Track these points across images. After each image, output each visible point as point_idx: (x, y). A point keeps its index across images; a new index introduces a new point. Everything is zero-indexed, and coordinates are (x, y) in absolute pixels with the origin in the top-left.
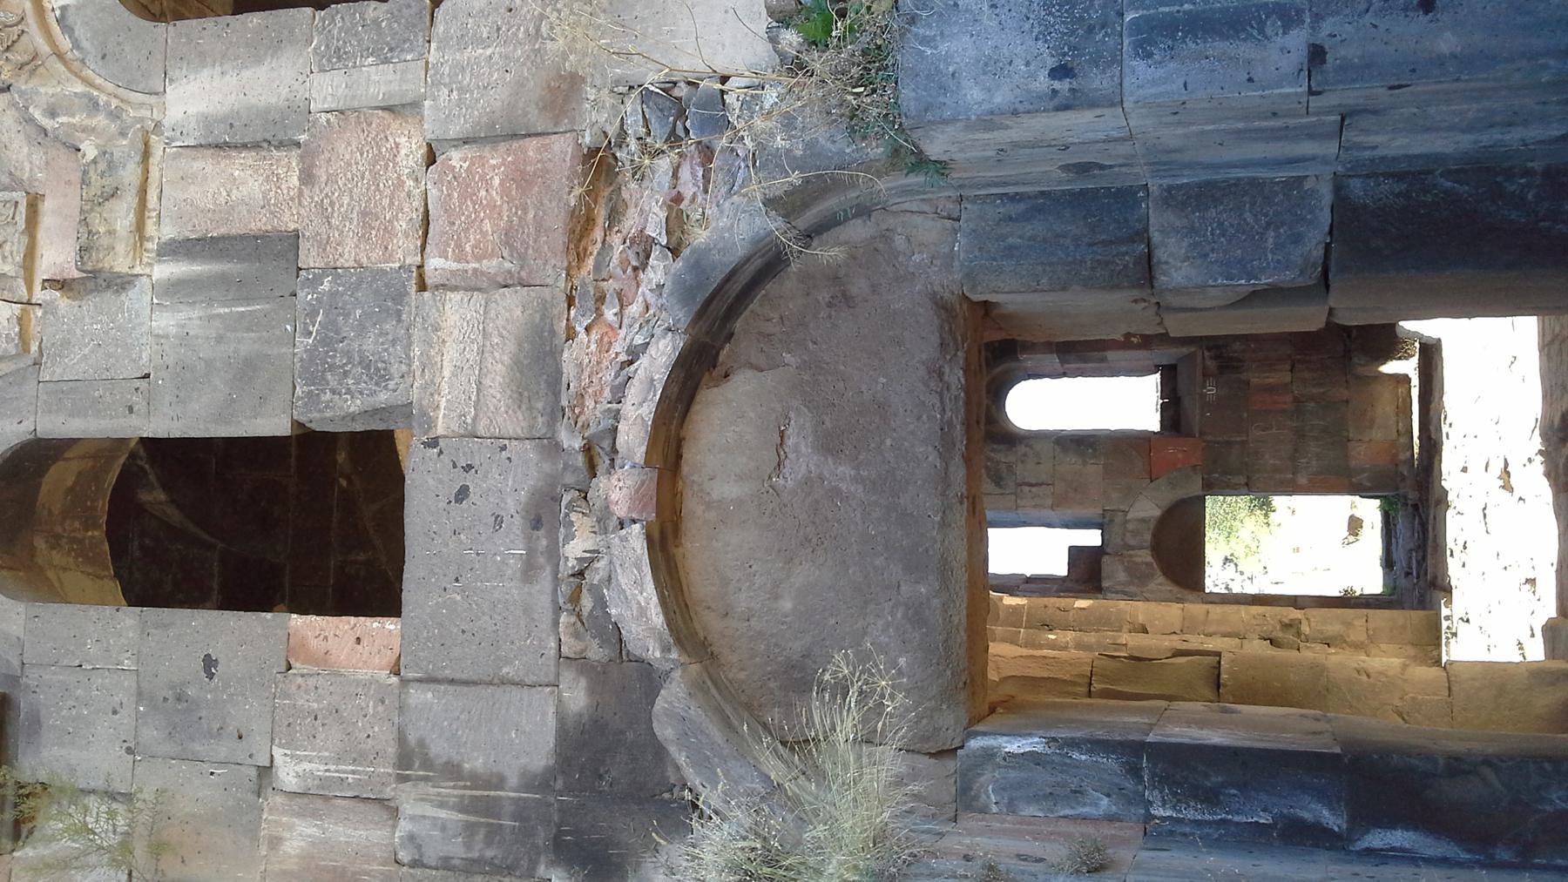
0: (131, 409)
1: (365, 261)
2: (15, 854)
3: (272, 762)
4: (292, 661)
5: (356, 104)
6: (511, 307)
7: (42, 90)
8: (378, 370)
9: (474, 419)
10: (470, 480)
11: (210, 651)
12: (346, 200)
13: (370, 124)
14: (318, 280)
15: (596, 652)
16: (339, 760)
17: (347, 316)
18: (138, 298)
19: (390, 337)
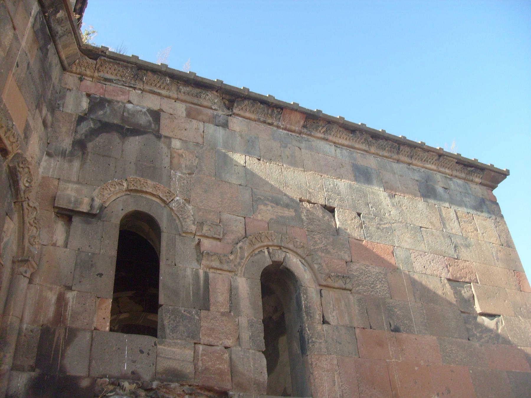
0: (167, 260)
1: (202, 328)
2: (53, 213)
3: (73, 290)
4: (100, 299)
5: (240, 329)
6: (189, 369)
7: (246, 246)
9: (161, 357)
10: (145, 354)
11: (104, 275)
12: (217, 324)
13: (235, 332)
14: (198, 315)
15: (97, 388)
16: (72, 310)
17: (189, 322)
18: (195, 265)
19: (183, 334)
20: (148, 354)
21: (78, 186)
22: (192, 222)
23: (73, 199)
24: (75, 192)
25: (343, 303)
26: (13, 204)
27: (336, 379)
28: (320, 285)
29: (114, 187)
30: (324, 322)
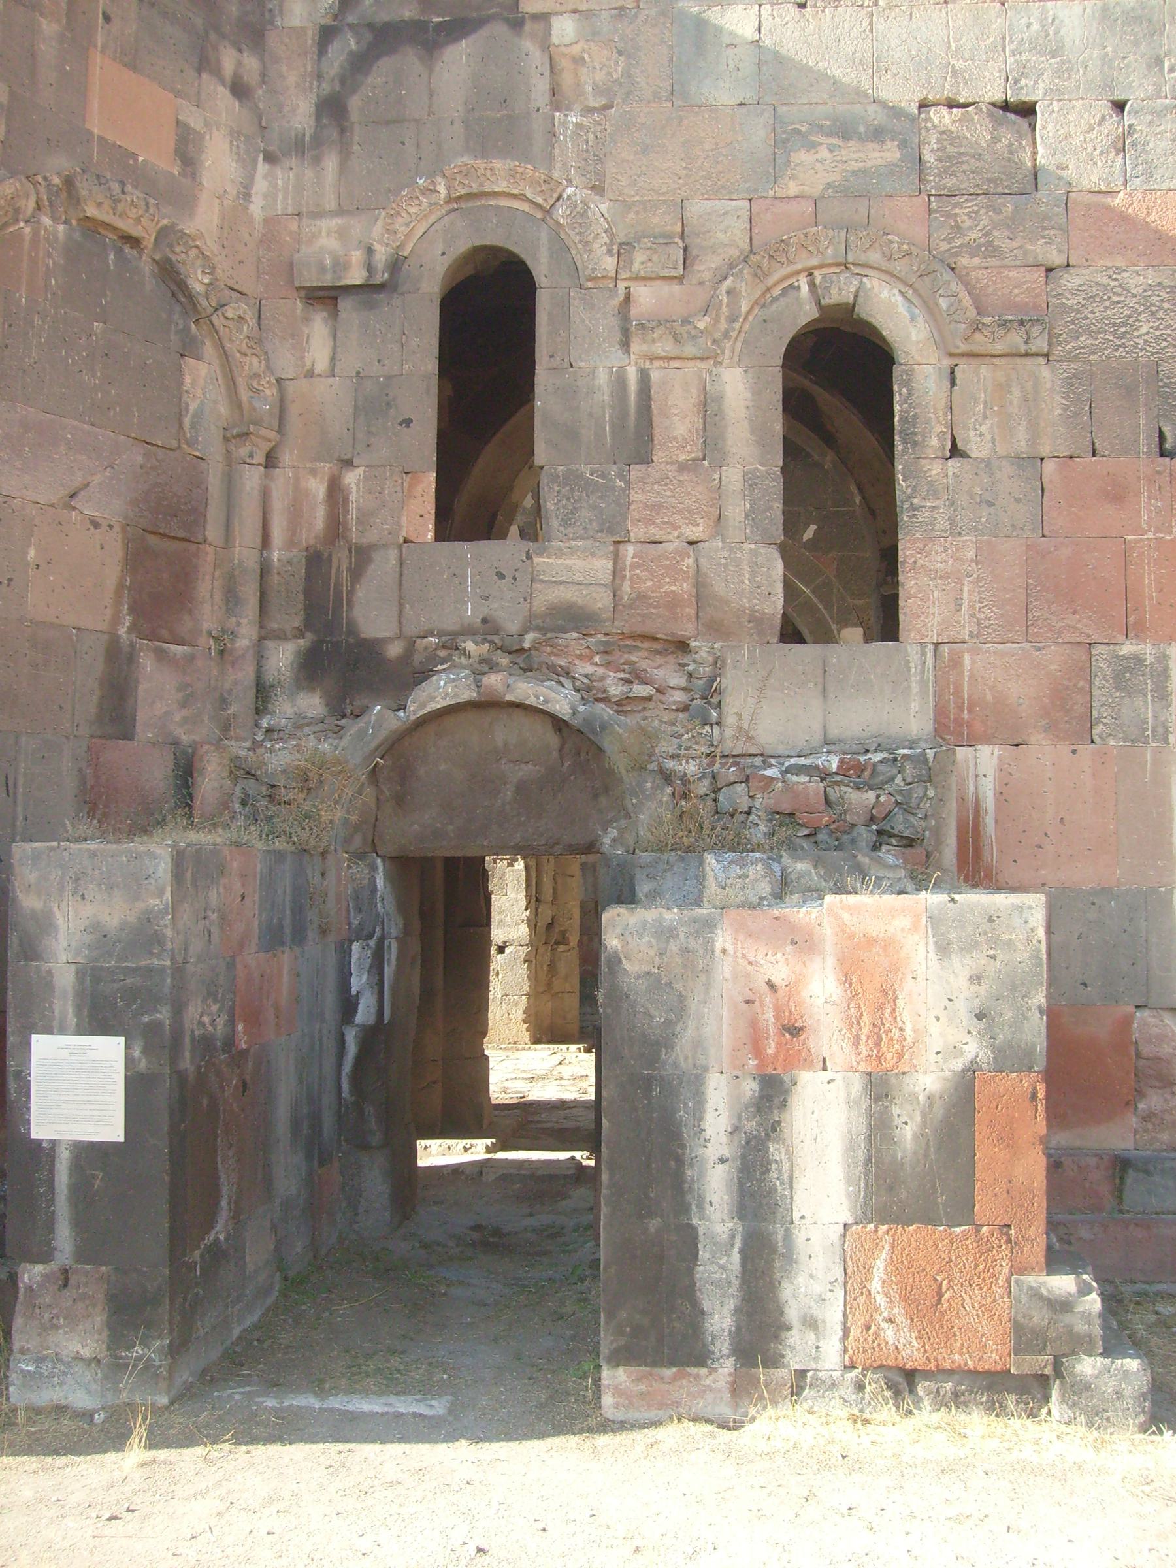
0: (552, 356)
1: (632, 507)
4: (410, 475)
5: (723, 497)
6: (601, 601)
7: (743, 284)
8: (570, 519)
9: (542, 581)
10: (508, 579)
12: (668, 493)
13: (711, 506)
15: (418, 658)
16: (358, 509)
17: (601, 498)
18: (616, 357)
20: (515, 579)
21: (339, 221)
22: (604, 248)
23: (328, 261)
24: (336, 239)
25: (1016, 393)
26: (193, 326)
27: (965, 596)
28: (951, 355)
29: (417, 202)
30: (955, 451)
